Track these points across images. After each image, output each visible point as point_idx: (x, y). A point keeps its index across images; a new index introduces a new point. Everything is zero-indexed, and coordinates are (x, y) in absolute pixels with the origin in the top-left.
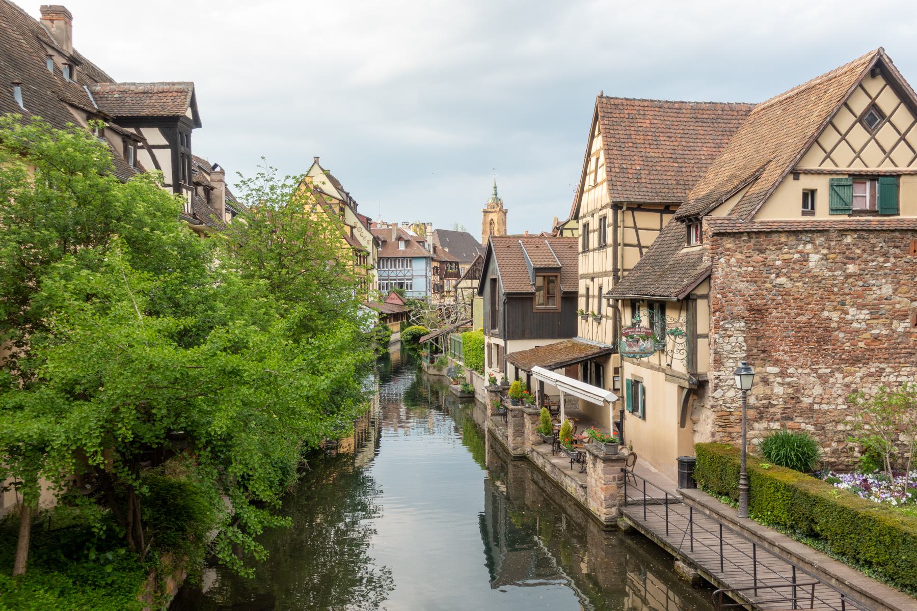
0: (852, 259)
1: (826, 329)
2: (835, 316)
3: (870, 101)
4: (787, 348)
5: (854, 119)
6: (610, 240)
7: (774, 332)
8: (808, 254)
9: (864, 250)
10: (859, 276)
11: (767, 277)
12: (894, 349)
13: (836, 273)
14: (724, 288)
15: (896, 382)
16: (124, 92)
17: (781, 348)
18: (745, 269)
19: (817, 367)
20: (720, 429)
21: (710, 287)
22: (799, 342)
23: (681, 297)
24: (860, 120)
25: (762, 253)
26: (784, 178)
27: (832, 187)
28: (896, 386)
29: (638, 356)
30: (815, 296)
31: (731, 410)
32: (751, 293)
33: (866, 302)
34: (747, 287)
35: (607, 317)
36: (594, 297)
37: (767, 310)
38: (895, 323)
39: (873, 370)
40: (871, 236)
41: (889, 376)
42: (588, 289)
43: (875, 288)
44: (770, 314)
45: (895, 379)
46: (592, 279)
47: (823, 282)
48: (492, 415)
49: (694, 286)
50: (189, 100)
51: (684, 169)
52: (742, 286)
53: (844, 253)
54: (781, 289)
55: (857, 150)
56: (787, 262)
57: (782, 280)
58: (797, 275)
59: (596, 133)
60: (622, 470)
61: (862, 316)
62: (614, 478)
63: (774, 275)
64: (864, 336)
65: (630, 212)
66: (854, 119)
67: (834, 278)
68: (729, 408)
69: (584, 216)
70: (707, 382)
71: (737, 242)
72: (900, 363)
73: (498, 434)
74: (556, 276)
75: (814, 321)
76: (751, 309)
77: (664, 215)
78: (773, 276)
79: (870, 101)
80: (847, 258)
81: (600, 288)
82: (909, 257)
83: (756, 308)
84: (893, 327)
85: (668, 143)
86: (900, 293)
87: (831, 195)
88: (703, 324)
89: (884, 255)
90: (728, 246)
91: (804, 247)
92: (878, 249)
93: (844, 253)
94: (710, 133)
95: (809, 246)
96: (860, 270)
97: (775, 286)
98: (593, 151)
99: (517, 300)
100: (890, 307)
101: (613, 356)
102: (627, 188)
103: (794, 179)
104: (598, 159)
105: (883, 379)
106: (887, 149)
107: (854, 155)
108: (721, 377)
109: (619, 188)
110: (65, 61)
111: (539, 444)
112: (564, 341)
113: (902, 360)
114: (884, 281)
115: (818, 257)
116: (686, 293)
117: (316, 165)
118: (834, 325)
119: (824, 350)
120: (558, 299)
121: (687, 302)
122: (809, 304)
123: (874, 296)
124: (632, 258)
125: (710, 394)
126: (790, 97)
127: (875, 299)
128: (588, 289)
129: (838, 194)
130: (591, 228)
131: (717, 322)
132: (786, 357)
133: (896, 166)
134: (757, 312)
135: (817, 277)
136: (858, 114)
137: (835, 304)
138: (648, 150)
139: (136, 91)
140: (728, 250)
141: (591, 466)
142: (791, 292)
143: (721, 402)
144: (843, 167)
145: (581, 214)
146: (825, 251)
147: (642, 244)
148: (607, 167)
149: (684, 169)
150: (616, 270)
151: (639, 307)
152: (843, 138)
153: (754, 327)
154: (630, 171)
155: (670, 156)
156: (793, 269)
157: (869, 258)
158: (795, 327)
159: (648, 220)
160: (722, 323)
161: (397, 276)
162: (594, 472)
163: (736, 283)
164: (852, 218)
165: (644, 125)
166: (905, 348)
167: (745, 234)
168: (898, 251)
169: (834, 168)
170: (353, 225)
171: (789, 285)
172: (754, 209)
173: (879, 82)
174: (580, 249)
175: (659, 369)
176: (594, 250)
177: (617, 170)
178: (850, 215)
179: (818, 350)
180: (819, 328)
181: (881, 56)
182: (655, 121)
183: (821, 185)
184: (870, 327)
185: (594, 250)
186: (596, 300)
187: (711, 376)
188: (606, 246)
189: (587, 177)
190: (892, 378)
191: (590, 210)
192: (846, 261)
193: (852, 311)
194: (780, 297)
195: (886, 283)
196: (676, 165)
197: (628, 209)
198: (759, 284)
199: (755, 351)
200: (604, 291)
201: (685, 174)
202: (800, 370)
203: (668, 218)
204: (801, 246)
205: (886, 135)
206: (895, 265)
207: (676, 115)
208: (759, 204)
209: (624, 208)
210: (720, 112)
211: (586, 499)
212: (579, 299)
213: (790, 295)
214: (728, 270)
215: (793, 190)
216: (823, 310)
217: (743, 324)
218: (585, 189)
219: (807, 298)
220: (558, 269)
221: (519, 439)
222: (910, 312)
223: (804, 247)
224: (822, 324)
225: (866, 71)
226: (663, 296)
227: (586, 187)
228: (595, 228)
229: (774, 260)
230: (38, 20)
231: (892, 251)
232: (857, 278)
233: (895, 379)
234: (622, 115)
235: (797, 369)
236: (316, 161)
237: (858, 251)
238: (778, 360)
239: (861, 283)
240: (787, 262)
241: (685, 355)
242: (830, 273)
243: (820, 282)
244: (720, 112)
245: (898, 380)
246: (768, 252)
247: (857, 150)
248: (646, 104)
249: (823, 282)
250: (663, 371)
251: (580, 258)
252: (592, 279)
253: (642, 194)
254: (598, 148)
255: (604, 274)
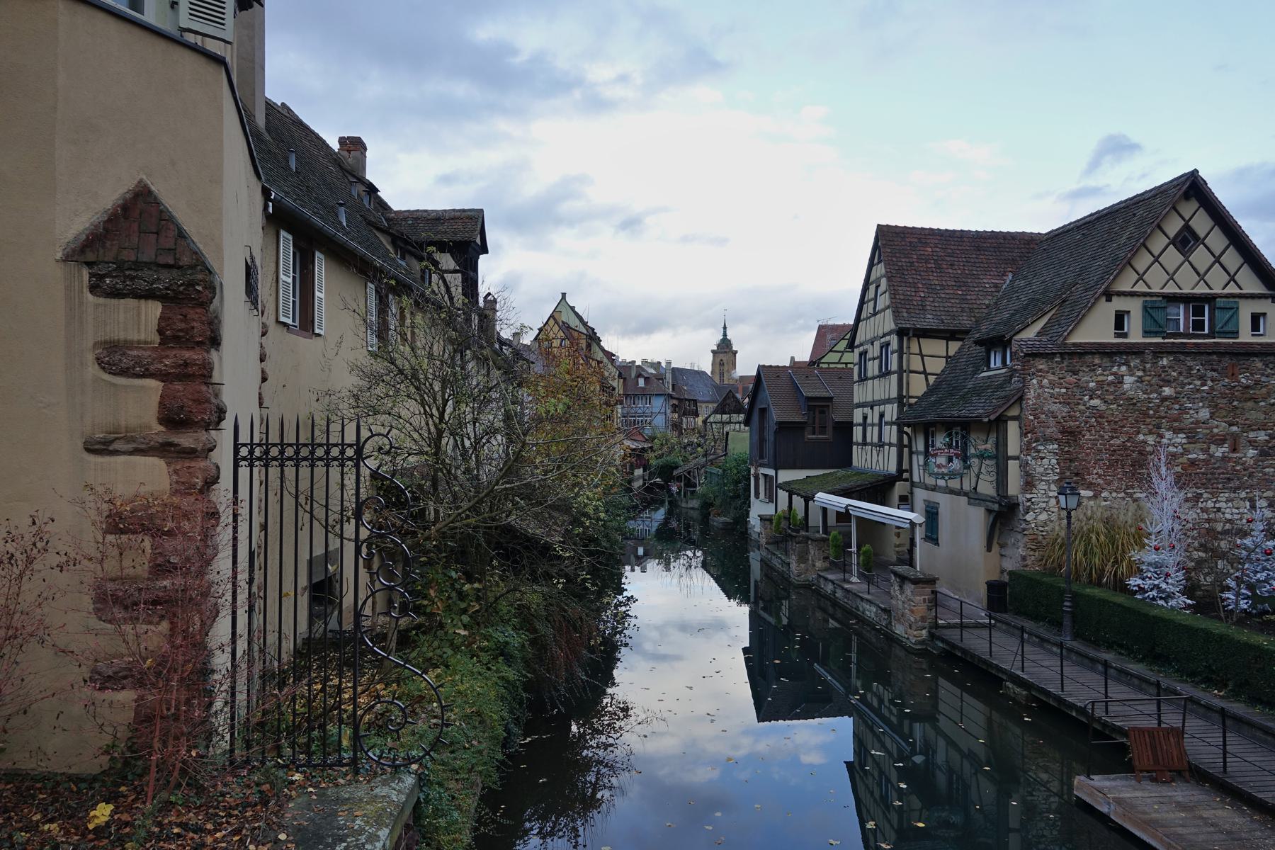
0: (1167, 382)
1: (1141, 453)
2: (1151, 439)
3: (1183, 223)
4: (1100, 471)
5: (1168, 241)
6: (894, 366)
7: (1087, 455)
8: (1123, 376)
9: (1180, 373)
10: (1175, 399)
11: (1081, 399)
12: (1211, 474)
13: (1151, 396)
14: (1036, 409)
15: (1214, 507)
16: (417, 219)
17: (1095, 471)
18: (1058, 390)
19: (1132, 491)
20: (1032, 553)
21: (1022, 409)
22: (1113, 465)
23: (992, 417)
24: (1173, 242)
25: (1075, 375)
26: (1097, 299)
27: (1145, 308)
28: (1215, 512)
29: (946, 478)
30: (1130, 419)
31: (1044, 533)
32: (1064, 414)
33: (1182, 425)
34: (1059, 409)
35: (890, 445)
36: (873, 425)
37: (1080, 432)
38: (1213, 447)
39: (1190, 495)
40: (1188, 359)
41: (1206, 501)
42: (865, 418)
43: (1191, 412)
44: (1083, 436)
45: (1213, 505)
46: (872, 408)
47: (1139, 405)
48: (767, 543)
49: (1005, 407)
50: (479, 226)
51: (969, 297)
52: (1054, 407)
53: (1160, 375)
54: (1095, 411)
55: (1171, 272)
56: (1100, 384)
57: (1096, 402)
58: (1112, 397)
59: (876, 261)
60: (933, 592)
61: (1179, 440)
62: (924, 599)
63: (1087, 397)
64: (1180, 460)
65: (916, 339)
66: (1168, 241)
67: (1150, 400)
68: (1042, 531)
69: (861, 345)
70: (1018, 504)
71: (1050, 363)
72: (1218, 488)
73: (776, 563)
74: (828, 406)
75: (1129, 444)
76: (1064, 431)
77: (950, 343)
78: (1086, 398)
79: (1183, 223)
80: (1163, 380)
81: (882, 416)
82: (1227, 380)
83: (1069, 430)
84: (1211, 451)
85: (951, 271)
86: (1217, 417)
87: (1144, 317)
88: (1013, 447)
89: (1202, 378)
90: (1041, 367)
91: (1119, 369)
92: (1195, 371)
93: (1160, 375)
94: (993, 261)
95: (1124, 368)
96: (1176, 393)
97: (1088, 408)
98: (872, 279)
99: (784, 428)
100: (1208, 431)
101: (898, 483)
102: (913, 315)
103: (1107, 301)
104: (877, 287)
105: (1200, 505)
106: (1202, 272)
107: (1168, 277)
108: (1033, 500)
109: (905, 315)
110: (364, 189)
111: (826, 570)
112: (840, 472)
113: (1220, 486)
114: (1201, 404)
115: (1133, 379)
116: (997, 414)
117: (563, 301)
118: (1148, 449)
119: (1139, 473)
120: (830, 429)
121: (997, 425)
122: (1124, 427)
123: (1191, 420)
124: (918, 386)
125: (1021, 517)
126: (1089, 222)
127: (1192, 423)
128: (865, 418)
129: (1152, 317)
130: (870, 355)
131: (1029, 443)
132: (1100, 481)
133: (1211, 289)
134: (1070, 435)
135: (1132, 399)
136: (1172, 235)
137: (1150, 427)
138: (931, 278)
139: (429, 217)
140: (1040, 371)
141: (897, 588)
142: (1106, 415)
143: (1033, 525)
144: (1156, 290)
145: (857, 342)
146: (1140, 373)
147: (928, 371)
148: (890, 294)
149: (969, 297)
150: (900, 398)
151: (933, 432)
152: (1156, 260)
153: (1066, 449)
154: (915, 298)
155: (954, 283)
156: (1107, 391)
157: (1186, 381)
158: (1110, 450)
159: (935, 347)
160: (1034, 445)
161: (636, 413)
162: (901, 594)
163: (1049, 404)
164: (1166, 341)
165: (926, 253)
166: (1223, 473)
167: (1058, 355)
168: (1215, 374)
169: (1146, 290)
170: (599, 359)
171: (1103, 407)
172: (1065, 331)
173: (1194, 204)
174: (856, 377)
175: (959, 493)
176: (873, 378)
177: (902, 297)
178: (1163, 338)
179: (1133, 474)
180: (1134, 452)
181: (1196, 178)
182: (938, 250)
183: (1134, 307)
184: (1186, 451)
185: (873, 378)
186: (876, 429)
187: (1021, 499)
188: (888, 373)
189: (865, 306)
190: (1210, 504)
191: (868, 338)
192: (1162, 383)
193: (1168, 434)
194: (1094, 420)
195: (1203, 407)
196: (960, 293)
197: (914, 336)
198: (1072, 405)
199: (1068, 474)
200: (887, 418)
201: (971, 302)
202: (1114, 494)
203: (954, 347)
204: (1116, 368)
205: (1200, 257)
206: (1212, 388)
207: (957, 243)
208: (1070, 325)
209: (911, 334)
210: (1002, 241)
211: (890, 623)
212: (854, 428)
213: (1104, 418)
214: (1040, 391)
215: (1103, 314)
216: (1138, 433)
217: (1056, 446)
218: (862, 317)
219: (1122, 420)
220: (830, 399)
221: (802, 565)
222: (1228, 437)
223: (1119, 369)
224: (1137, 447)
225: (1181, 192)
226: (971, 417)
227: (864, 315)
228: (875, 355)
229: (1089, 382)
230: (336, 151)
231: (1210, 374)
232: (1173, 401)
233: (1213, 505)
234: (903, 243)
235: (1111, 493)
236: (564, 295)
237: (1174, 374)
238: (1091, 484)
239: (1177, 407)
240: (1100, 384)
241: (994, 478)
242: (1146, 396)
243: (1135, 404)
244: (1002, 241)
245: (1217, 506)
246: (1081, 374)
247: (1171, 272)
248: (927, 232)
249: (1139, 405)
250: (966, 494)
251: (856, 386)
252: (872, 408)
253: (927, 320)
254: (879, 275)
255: (888, 401)
